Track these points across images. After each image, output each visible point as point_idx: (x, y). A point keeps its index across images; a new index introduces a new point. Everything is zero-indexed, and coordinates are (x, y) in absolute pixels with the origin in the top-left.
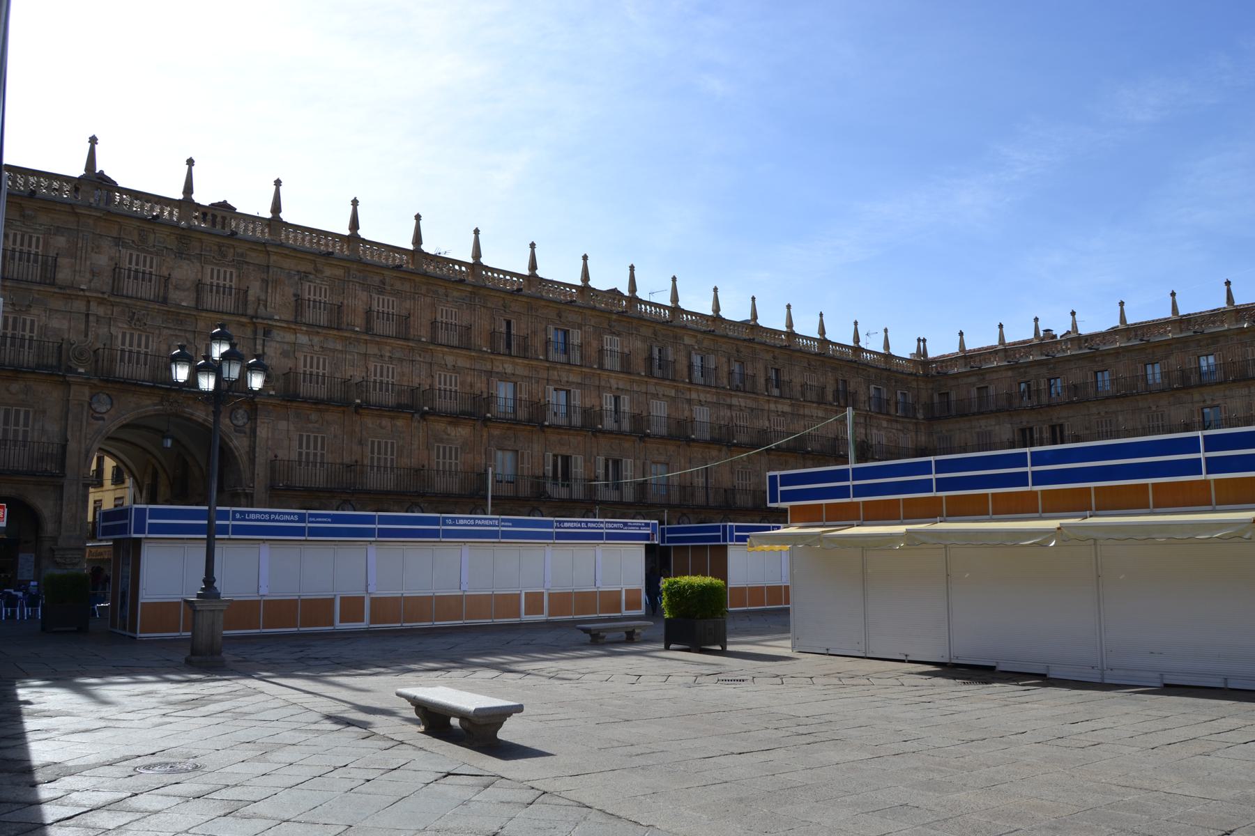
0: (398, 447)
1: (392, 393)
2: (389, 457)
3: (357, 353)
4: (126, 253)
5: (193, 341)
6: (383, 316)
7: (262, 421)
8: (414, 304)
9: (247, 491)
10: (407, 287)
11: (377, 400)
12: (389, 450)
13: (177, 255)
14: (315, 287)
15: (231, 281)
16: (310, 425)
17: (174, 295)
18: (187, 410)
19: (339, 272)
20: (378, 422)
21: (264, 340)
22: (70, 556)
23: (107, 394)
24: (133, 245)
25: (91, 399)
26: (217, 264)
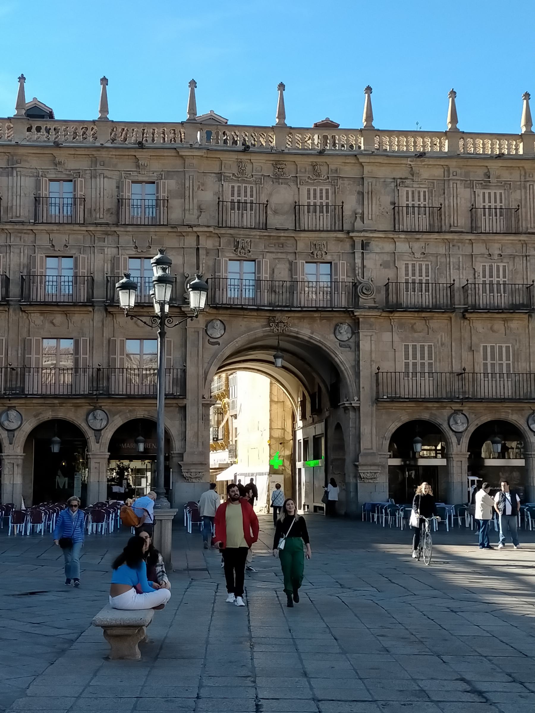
0: (514, 351)
1: (504, 292)
2: (504, 362)
3: (462, 255)
4: (229, 186)
6: (496, 213)
7: (365, 334)
8: (526, 193)
9: (353, 405)
10: (516, 176)
11: (488, 302)
13: (275, 180)
14: (413, 193)
15: (327, 198)
16: (416, 335)
17: (274, 221)
18: (292, 329)
19: (438, 172)
20: (489, 325)
21: (363, 253)
22: (194, 470)
23: (220, 321)
24: (234, 178)
25: (206, 326)
26: (313, 184)
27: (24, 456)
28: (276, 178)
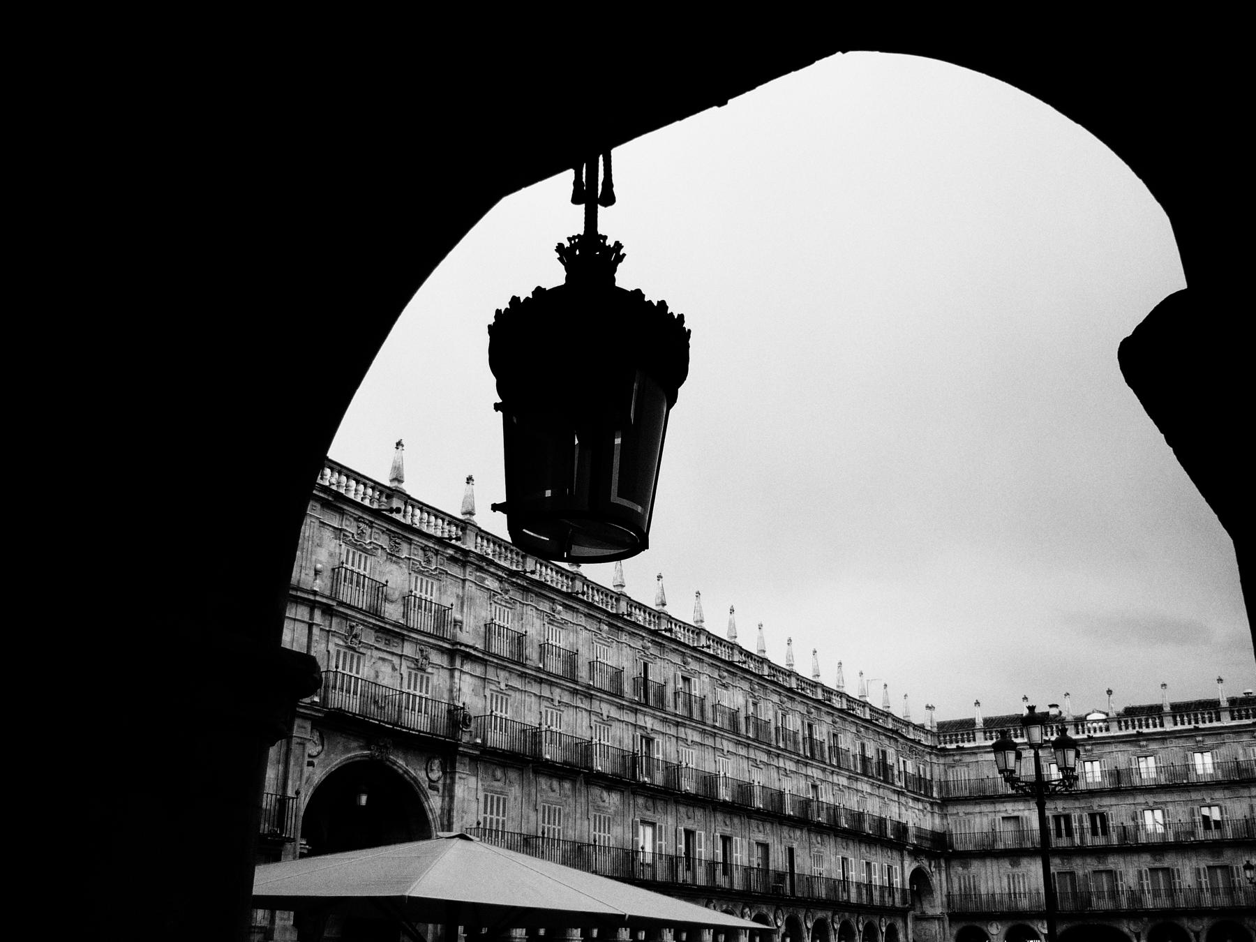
5: (398, 668)
12: (557, 821)
13: (389, 556)
27: (527, 939)
28: (391, 554)
